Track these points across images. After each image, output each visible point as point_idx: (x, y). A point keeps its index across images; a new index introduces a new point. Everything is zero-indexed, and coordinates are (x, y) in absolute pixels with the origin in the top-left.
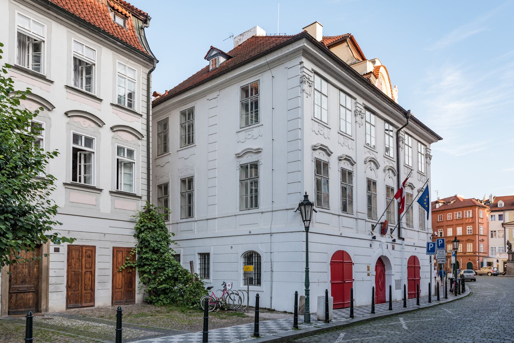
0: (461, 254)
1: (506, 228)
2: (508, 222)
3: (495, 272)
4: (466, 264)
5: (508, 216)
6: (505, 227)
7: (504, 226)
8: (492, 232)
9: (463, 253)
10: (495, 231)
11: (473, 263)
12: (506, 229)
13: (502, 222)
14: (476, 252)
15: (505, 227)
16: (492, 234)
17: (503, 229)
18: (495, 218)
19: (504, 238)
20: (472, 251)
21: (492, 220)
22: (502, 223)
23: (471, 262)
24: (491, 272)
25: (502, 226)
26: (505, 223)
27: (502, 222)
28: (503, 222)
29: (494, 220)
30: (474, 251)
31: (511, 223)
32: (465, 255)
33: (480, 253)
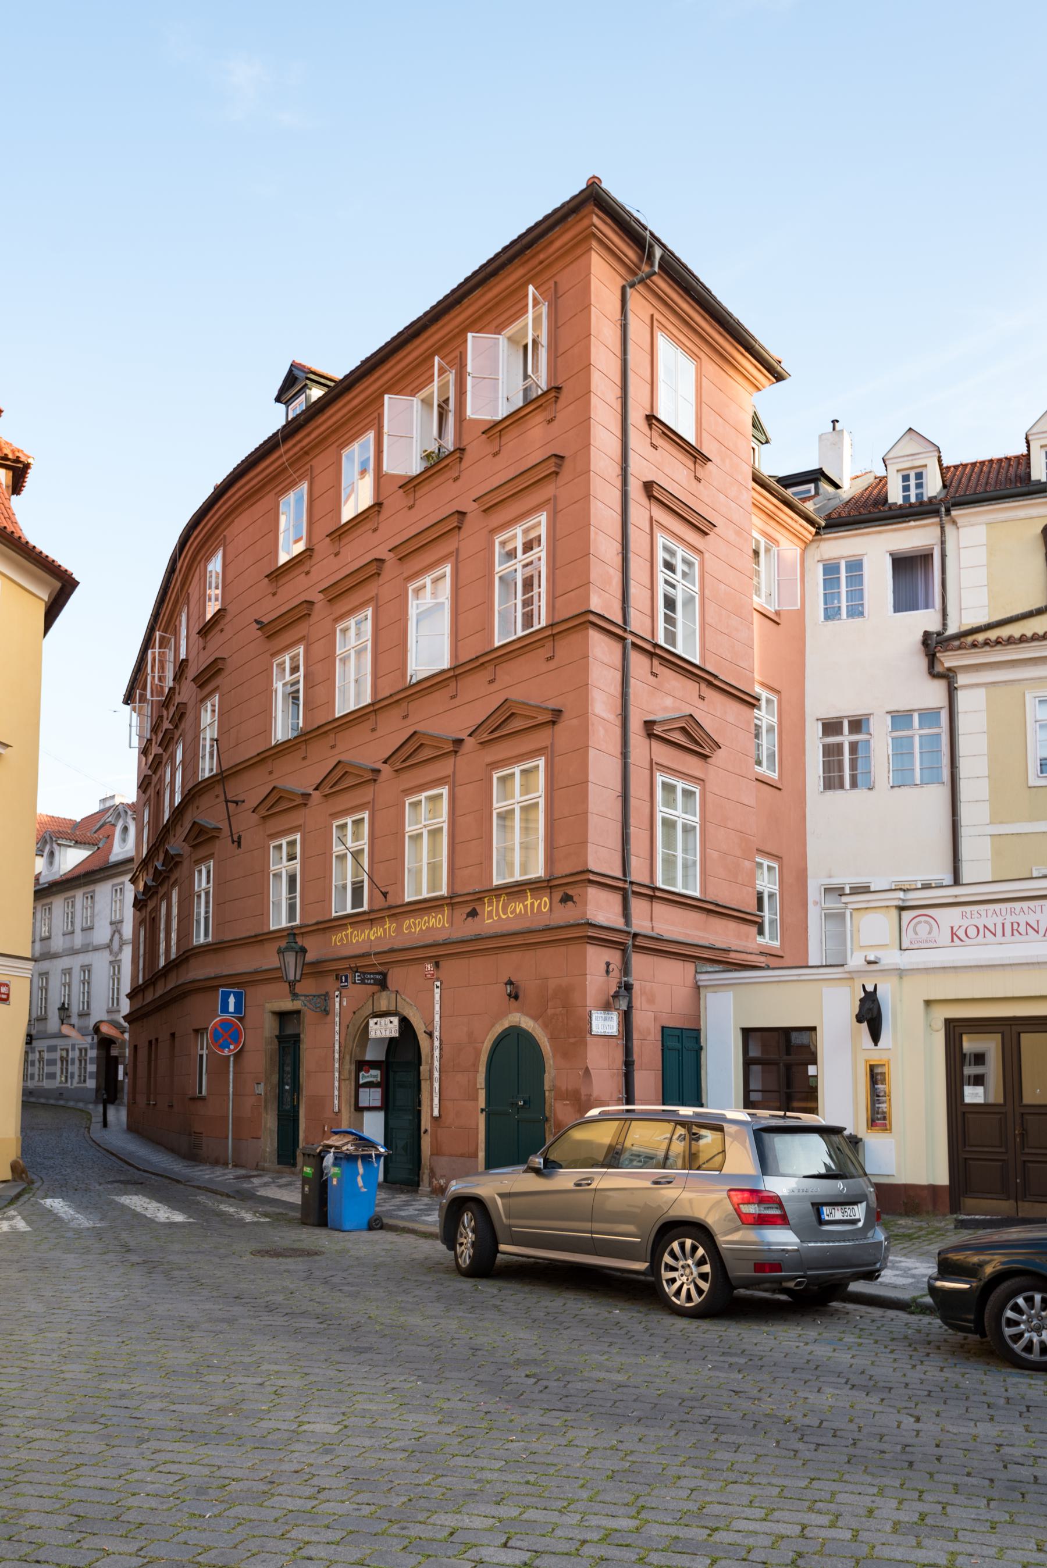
0: (437, 924)
1: (962, 679)
2: (982, 619)
3: (783, 1238)
4: (475, 1066)
5: (980, 556)
6: (948, 677)
7: (948, 660)
8: (831, 727)
9: (451, 902)
10: (857, 725)
11: (552, 1039)
12: (961, 696)
13: (926, 620)
14: (586, 878)
15: (948, 677)
16: (832, 752)
17: (934, 694)
18: (856, 594)
19: (944, 792)
20: (538, 871)
21: (831, 614)
22: (927, 635)
23: (527, 1023)
24: (700, 1231)
25: (923, 663)
26: (952, 630)
27: (926, 620)
28: (934, 627)
29: (856, 611)
30: (564, 868)
31: (1004, 632)
32: (469, 928)
33: (654, 895)
